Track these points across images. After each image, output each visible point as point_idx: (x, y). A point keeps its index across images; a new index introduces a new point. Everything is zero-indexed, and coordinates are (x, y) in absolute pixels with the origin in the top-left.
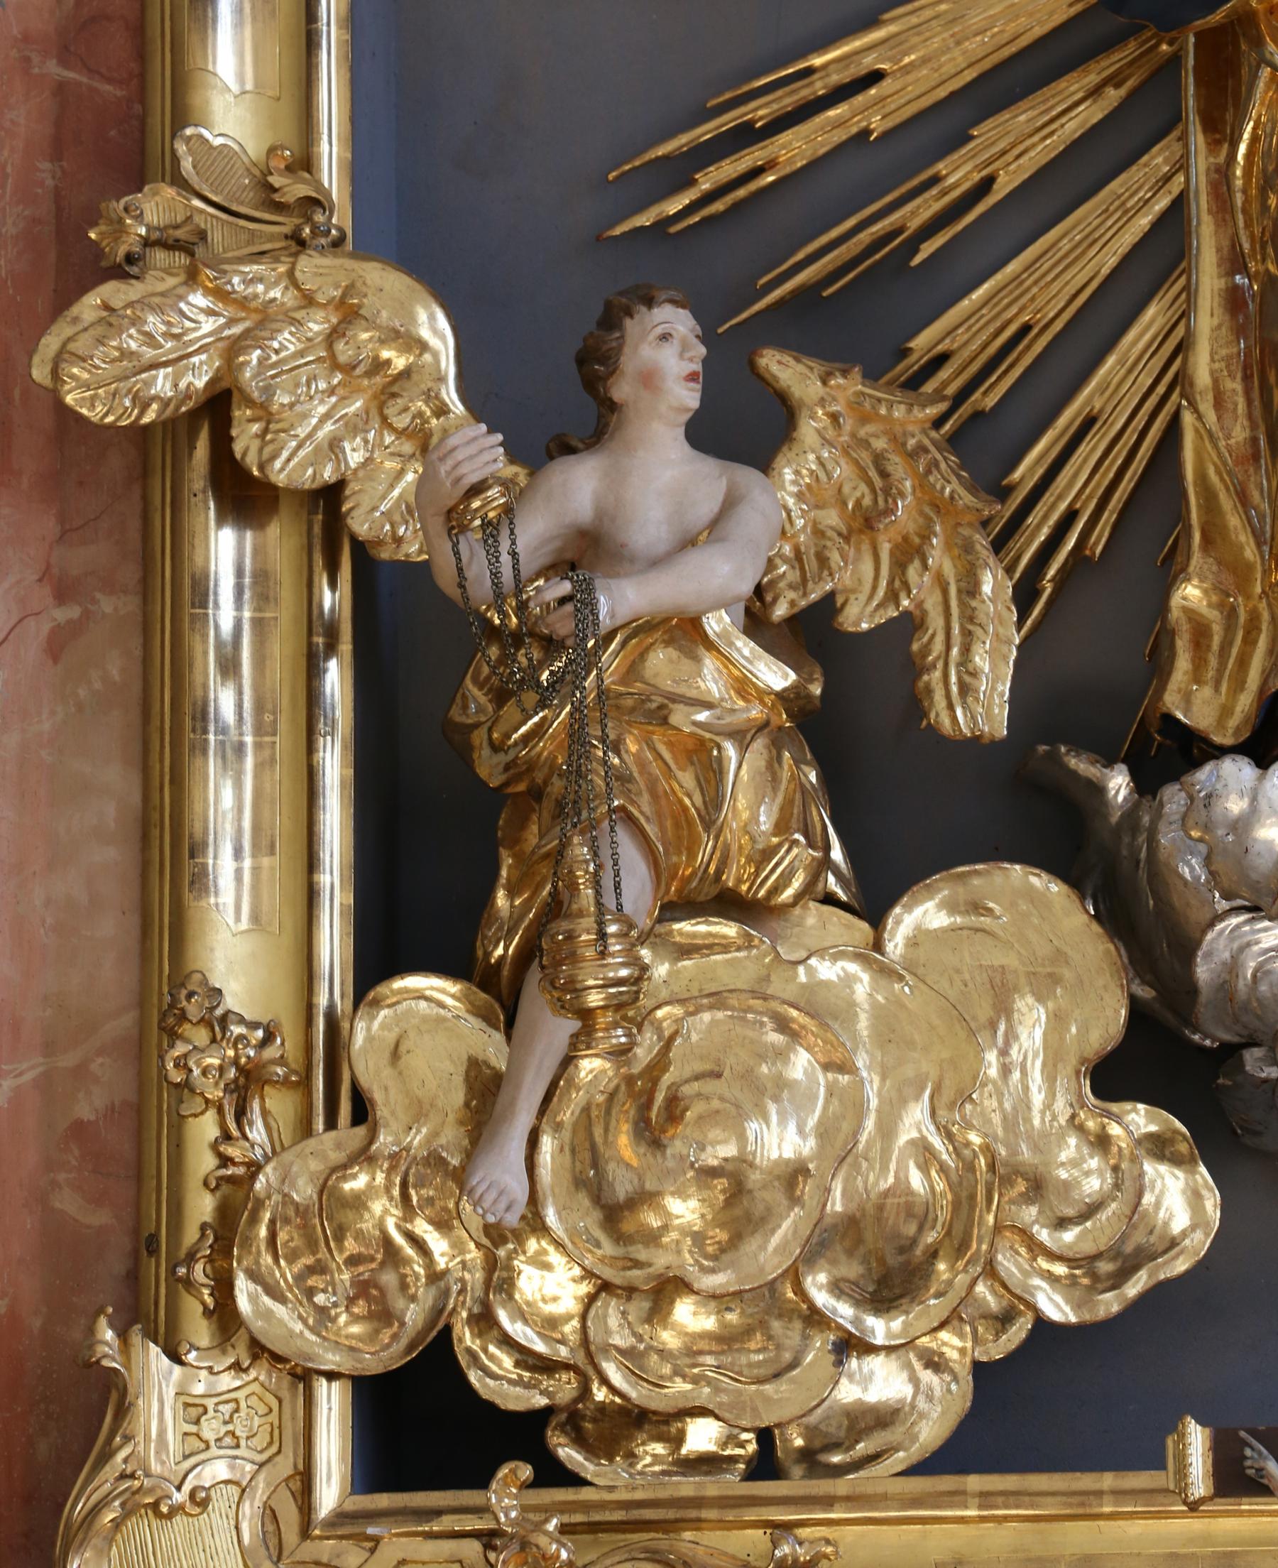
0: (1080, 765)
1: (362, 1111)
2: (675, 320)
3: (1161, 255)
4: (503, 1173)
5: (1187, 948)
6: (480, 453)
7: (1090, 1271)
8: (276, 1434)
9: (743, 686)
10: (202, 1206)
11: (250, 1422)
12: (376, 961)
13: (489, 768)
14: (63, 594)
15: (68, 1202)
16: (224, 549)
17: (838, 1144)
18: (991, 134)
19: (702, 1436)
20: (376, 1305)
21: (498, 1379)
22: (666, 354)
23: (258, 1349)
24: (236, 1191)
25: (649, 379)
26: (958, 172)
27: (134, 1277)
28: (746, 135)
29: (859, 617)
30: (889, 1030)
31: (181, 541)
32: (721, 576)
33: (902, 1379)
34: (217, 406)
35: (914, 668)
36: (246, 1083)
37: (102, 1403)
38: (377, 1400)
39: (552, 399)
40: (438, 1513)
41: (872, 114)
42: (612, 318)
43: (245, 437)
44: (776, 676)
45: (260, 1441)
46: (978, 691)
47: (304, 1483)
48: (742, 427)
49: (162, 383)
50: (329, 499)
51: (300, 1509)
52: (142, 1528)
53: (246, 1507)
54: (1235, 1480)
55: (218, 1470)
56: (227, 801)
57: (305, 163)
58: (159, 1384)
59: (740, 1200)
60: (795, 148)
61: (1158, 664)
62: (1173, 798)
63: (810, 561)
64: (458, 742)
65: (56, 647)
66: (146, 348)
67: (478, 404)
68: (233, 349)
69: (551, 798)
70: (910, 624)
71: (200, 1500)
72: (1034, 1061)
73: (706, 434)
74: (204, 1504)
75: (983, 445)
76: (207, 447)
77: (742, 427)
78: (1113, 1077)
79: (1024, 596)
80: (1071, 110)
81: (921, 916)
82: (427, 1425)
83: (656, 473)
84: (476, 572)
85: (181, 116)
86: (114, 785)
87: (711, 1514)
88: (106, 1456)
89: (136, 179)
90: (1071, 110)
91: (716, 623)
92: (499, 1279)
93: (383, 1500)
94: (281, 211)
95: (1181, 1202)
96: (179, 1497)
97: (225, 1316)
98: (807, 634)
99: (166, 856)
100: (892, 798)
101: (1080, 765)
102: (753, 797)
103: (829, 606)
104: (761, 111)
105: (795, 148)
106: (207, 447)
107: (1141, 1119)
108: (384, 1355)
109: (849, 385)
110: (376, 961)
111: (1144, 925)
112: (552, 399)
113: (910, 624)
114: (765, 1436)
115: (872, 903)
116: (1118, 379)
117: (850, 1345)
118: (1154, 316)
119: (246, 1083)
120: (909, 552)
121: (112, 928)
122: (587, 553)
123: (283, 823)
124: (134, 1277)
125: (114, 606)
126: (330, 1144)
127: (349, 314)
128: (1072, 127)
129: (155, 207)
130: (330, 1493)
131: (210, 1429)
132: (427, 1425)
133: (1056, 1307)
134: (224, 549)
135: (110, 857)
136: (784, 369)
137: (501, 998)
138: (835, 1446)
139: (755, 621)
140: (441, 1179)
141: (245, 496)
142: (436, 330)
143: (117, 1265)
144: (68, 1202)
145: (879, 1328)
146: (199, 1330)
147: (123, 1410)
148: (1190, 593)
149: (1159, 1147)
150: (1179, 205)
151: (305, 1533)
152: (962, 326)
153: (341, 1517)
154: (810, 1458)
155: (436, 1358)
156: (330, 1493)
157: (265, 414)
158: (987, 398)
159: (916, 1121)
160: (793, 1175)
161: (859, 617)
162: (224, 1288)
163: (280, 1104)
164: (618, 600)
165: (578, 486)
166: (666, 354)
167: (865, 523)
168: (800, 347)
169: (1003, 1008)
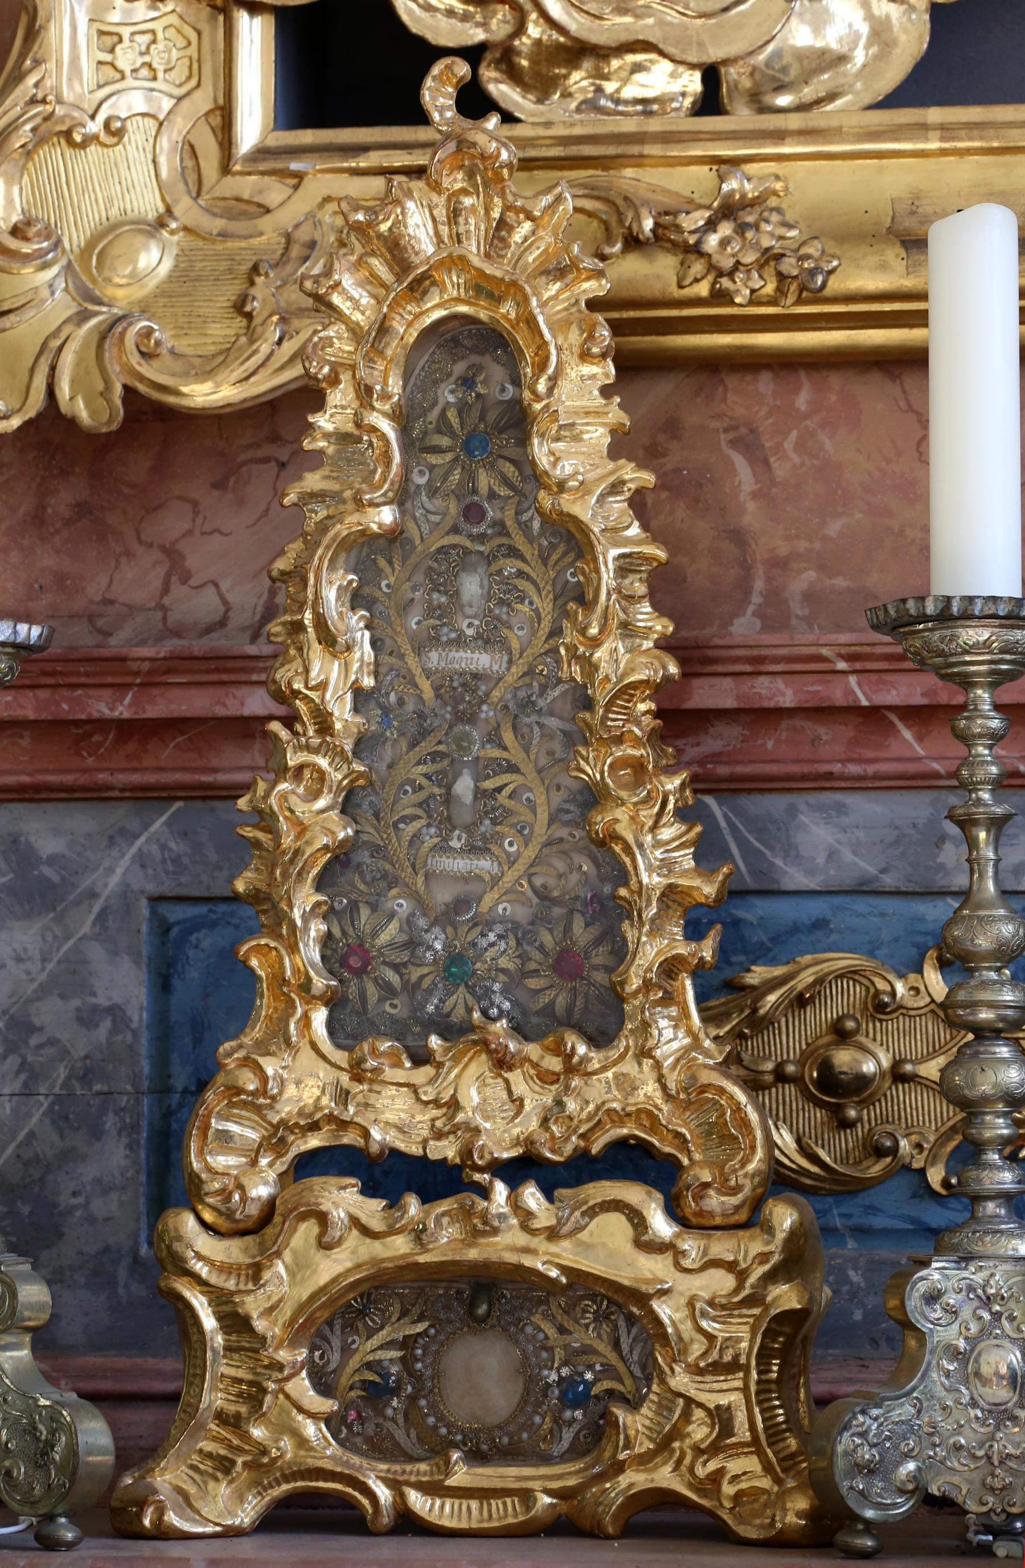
8: (195, 69)
40: (364, 149)
45: (180, 73)
47: (224, 117)
51: (221, 145)
53: (164, 142)
55: (131, 102)
71: (115, 130)
74: (119, 134)
87: (654, 150)
88: (18, 77)
93: (308, 136)
96: (95, 127)
114: (711, 75)
130: (252, 124)
131: (126, 58)
138: (780, 88)
147: (32, 34)
151: (225, 169)
153: (262, 152)
156: (252, 124)
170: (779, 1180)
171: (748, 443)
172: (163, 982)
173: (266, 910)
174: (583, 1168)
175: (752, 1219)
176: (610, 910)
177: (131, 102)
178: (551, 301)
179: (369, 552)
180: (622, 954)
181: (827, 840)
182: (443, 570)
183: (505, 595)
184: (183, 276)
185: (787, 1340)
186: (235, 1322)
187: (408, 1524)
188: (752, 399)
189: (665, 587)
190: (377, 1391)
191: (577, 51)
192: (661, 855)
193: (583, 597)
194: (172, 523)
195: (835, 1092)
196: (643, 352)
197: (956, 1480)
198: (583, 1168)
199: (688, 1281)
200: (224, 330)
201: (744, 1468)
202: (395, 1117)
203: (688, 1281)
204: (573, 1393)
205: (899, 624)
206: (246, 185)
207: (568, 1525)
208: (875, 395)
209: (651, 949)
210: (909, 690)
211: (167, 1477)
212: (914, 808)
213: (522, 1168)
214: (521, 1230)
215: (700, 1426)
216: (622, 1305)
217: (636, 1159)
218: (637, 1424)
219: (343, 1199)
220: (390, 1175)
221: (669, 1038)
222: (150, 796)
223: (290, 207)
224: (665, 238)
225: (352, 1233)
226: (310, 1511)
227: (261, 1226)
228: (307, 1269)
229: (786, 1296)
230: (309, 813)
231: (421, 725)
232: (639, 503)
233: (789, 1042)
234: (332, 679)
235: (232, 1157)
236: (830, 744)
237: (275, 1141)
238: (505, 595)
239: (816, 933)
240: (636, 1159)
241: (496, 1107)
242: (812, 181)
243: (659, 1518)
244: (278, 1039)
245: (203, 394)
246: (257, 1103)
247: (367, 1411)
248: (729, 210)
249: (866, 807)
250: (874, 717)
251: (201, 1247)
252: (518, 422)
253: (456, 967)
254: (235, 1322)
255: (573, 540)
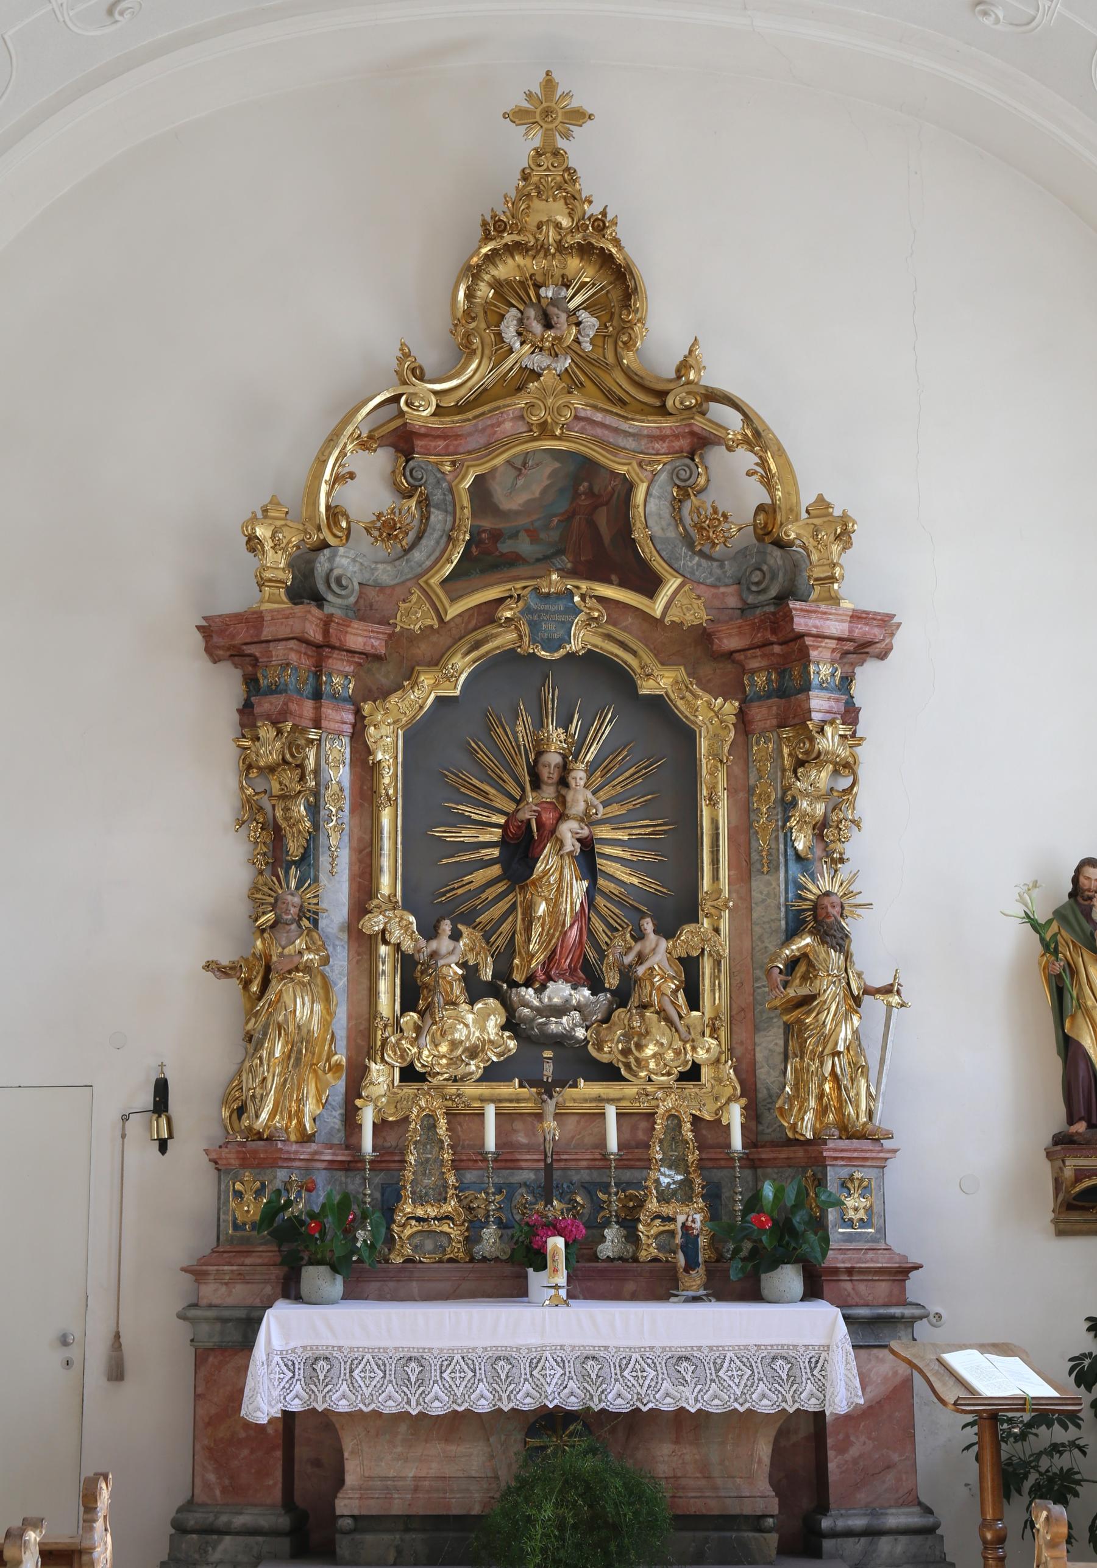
0: (499, 983)
1: (402, 1031)
2: (448, 922)
3: (513, 908)
4: (422, 1041)
5: (515, 1011)
6: (422, 942)
7: (499, 1055)
9: (455, 973)
10: (379, 1043)
11: (386, 1073)
12: (404, 1010)
13: (420, 984)
14: (359, 954)
15: (359, 1041)
16: (383, 950)
17: (468, 1037)
18: (488, 891)
19: (446, 1076)
20: (402, 1057)
21: (418, 1066)
22: (446, 926)
23: (387, 1063)
24: (385, 1042)
25: (444, 930)
26: (484, 896)
27: (368, 1052)
28: (454, 889)
29: (471, 963)
30: (475, 1021)
31: (377, 950)
32: (454, 958)
33: (475, 1067)
34: (383, 931)
35: (477, 970)
36: (385, 1026)
37: (366, 1069)
38: (401, 1069)
39: (430, 931)
41: (472, 887)
42: (439, 921)
43: (387, 936)
44: (460, 972)
46: (487, 974)
48: (456, 936)
49: (376, 928)
50: (398, 947)
52: (371, 1087)
54: (521, 1086)
56: (383, 986)
57: (395, 895)
58: (373, 1066)
59: (454, 1045)
60: (460, 891)
61: (511, 973)
62: (514, 990)
63: (464, 955)
64: (415, 980)
65: (358, 962)
66: (375, 923)
67: (420, 934)
68: (386, 923)
69: (432, 989)
70: (478, 964)
72: (493, 1025)
73: (450, 937)
75: (487, 937)
76: (383, 936)
77: (456, 936)
78: (504, 1028)
79: (492, 956)
80: (500, 888)
81: (479, 1005)
82: (410, 1074)
83: (444, 944)
84: (422, 957)
85: (378, 889)
86: (365, 983)
89: (371, 899)
90: (500, 888)
91: (453, 965)
92: (420, 1053)
94: (390, 898)
95: (512, 1044)
97: (383, 1060)
98: (463, 965)
99: (373, 993)
100: (475, 990)
101: (499, 983)
102: (457, 990)
103: (467, 961)
104: (456, 886)
105: (460, 891)
106: (383, 936)
107: (507, 1034)
108: (405, 1065)
109: (470, 930)
110: (404, 1010)
111: (509, 1008)
112: (430, 931)
113: (478, 964)
115: (472, 1002)
116: (505, 927)
117: (468, 1064)
118: (510, 919)
119: (385, 1026)
120: (478, 954)
121: (365, 1003)
122: (434, 955)
123: (391, 989)
124: (368, 1052)
125: (366, 957)
126: (399, 1035)
127: (402, 919)
128: (500, 890)
129: (375, 902)
132: (410, 1074)
133: (495, 1059)
134: (383, 950)
135: (365, 993)
136: (460, 926)
137: (422, 1014)
139: (457, 964)
140: (415, 1041)
141: (386, 942)
142: (412, 919)
143: (366, 1050)
144: (359, 1041)
145: (472, 1062)
146: (379, 1060)
148: (516, 961)
149: (509, 1037)
150: (515, 902)
152: (483, 918)
154: (462, 1079)
155: (412, 1064)
156: (397, 1082)
157: (390, 933)
158: (487, 928)
159: (477, 1034)
160: (461, 1042)
161: (471, 963)
162: (383, 1055)
163: (389, 1029)
164: (441, 963)
165: (434, 945)
166: (446, 926)
167: (472, 950)
168: (463, 924)
169: (489, 1015)
170: (465, 1221)
171: (460, 1124)
172: (383, 1195)
173: (404, 1187)
174: (442, 1219)
175: (462, 1224)
176: (445, 1187)
177: (381, 1079)
178: (438, 1112)
179: (416, 1143)
180: (447, 1193)
181: (470, 1176)
182: (425, 1145)
183: (432, 1148)
184: (388, 1102)
185: (467, 1239)
186: (400, 1238)
187: (421, 1262)
188: (461, 1119)
189: (452, 1147)
190: (416, 1247)
191: (438, 1073)
192: (452, 1180)
193: (442, 1148)
194: (384, 1134)
195: (470, 1209)
196: (449, 1114)
197: (487, 1254)
198: (442, 1219)
199: (455, 1232)
200: (393, 1110)
201: (461, 1255)
202: (420, 1212)
203: (455, 1232)
204: (441, 1246)
205: (481, 1154)
206: (395, 1090)
207: (440, 1261)
208: (476, 1118)
209: (451, 1192)
210: (480, 1157)
211: (391, 1256)
212: (480, 1172)
213: (435, 1219)
214: (435, 1226)
215: (457, 1249)
216: (448, 1234)
217: (447, 1218)
218: (448, 1249)
219: (413, 1222)
220: (419, 1220)
221: (453, 1203)
222: (382, 1170)
223: (401, 1093)
224: (450, 1099)
225: (414, 1227)
226: (409, 1260)
227: (404, 1226)
228: (408, 1232)
229: (466, 1234)
230: (409, 1175)
231: (423, 1163)
232: (450, 1137)
233: (465, 1203)
234: (412, 1159)
235: (399, 1218)
236: (470, 1164)
237: (405, 1215)
238: (432, 1148)
239: (468, 1188)
240: (447, 1218)
241: (432, 1212)
242: (470, 1090)
243: (451, 1260)
244: (405, 1203)
245: (391, 1119)
246: (403, 1211)
247: (415, 1248)
248: (459, 1095)
249: (475, 1172)
250: (476, 1161)
251: (396, 1228)
252: (435, 1126)
253: (426, 1194)
254: (400, 1238)
255: (442, 1142)
